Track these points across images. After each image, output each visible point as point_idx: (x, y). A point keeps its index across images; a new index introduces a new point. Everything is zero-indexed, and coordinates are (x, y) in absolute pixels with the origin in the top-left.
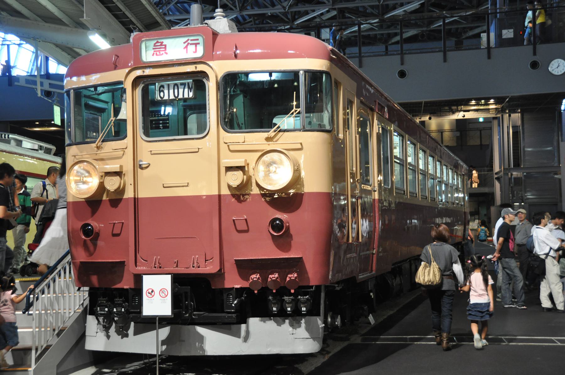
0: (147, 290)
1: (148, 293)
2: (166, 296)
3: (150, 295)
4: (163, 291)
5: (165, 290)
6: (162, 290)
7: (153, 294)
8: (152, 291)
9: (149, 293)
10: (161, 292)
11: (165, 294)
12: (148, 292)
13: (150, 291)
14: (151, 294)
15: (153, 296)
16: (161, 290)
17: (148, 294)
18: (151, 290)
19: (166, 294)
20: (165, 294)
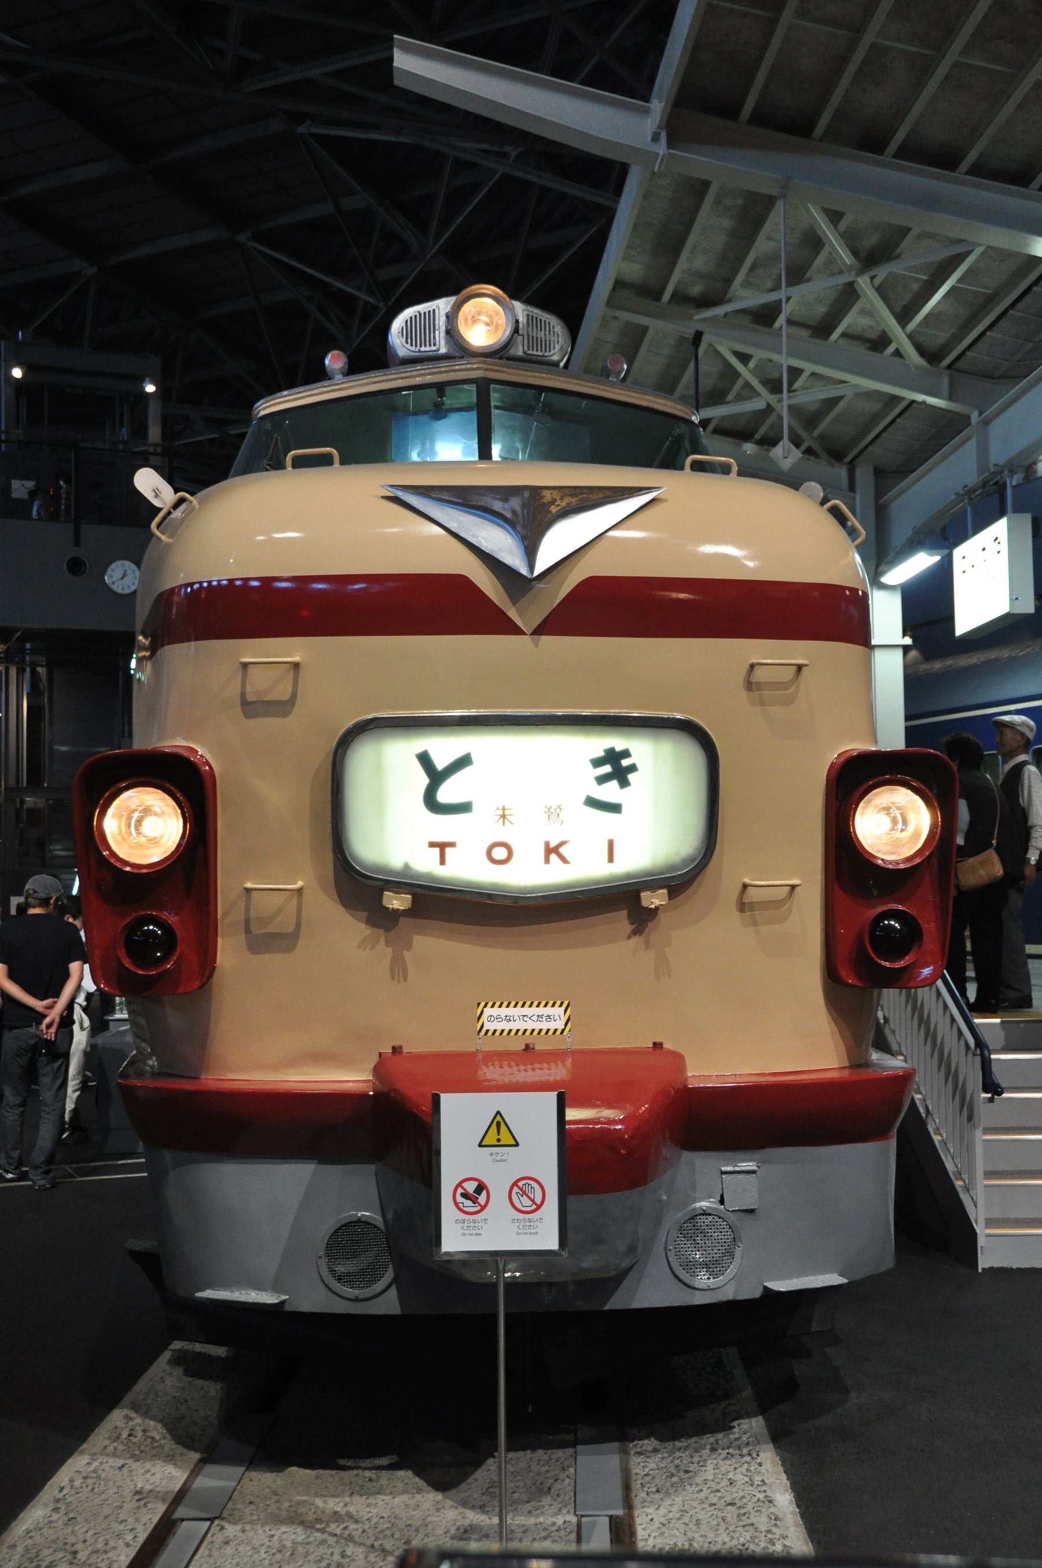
0: (460, 1185)
1: (463, 1195)
2: (539, 1207)
3: (468, 1203)
4: (526, 1189)
5: (530, 1182)
6: (520, 1184)
7: (482, 1199)
8: (481, 1188)
9: (465, 1195)
10: (516, 1190)
11: (533, 1201)
12: (460, 1191)
13: (471, 1187)
14: (474, 1200)
15: (483, 1208)
16: (515, 1184)
17: (460, 1199)
18: (475, 1184)
19: (538, 1201)
20: (533, 1201)
